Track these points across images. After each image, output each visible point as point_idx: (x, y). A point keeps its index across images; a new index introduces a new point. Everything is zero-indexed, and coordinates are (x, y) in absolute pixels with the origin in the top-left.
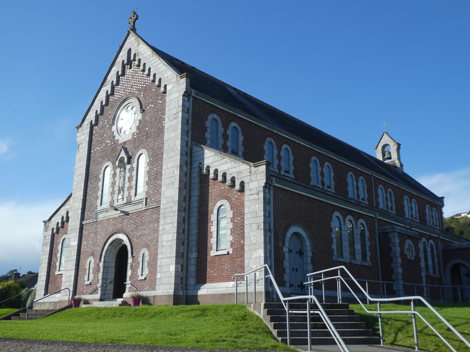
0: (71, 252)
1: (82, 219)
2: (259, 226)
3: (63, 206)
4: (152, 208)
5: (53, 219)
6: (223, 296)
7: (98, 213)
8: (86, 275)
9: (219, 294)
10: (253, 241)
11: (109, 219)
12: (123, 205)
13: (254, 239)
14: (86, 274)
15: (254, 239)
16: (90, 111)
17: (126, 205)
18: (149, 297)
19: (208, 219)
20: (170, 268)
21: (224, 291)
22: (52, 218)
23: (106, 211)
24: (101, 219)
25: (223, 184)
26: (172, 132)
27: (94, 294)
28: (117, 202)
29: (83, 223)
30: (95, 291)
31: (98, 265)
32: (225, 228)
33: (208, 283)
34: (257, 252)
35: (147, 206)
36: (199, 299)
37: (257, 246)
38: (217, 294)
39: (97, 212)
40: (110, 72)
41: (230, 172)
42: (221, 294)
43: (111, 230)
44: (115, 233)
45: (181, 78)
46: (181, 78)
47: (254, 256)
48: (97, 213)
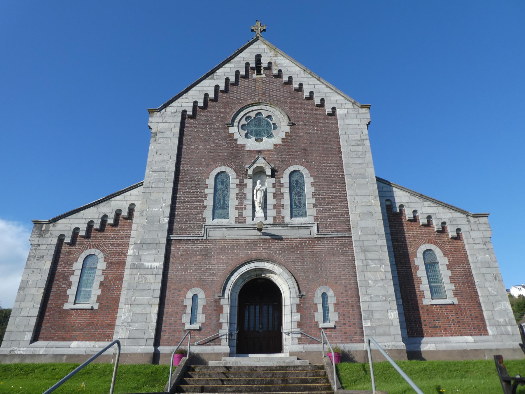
0: (146, 276)
1: (170, 231)
2: (497, 278)
3: (92, 206)
4: (330, 237)
5: (60, 221)
6: (464, 352)
7: (208, 229)
8: (184, 315)
9: (457, 350)
10: (491, 292)
11: (238, 239)
12: (269, 226)
13: (492, 289)
14: (185, 313)
15: (492, 289)
16: (180, 98)
17: (271, 226)
18: (349, 351)
19: (410, 263)
20: (389, 314)
21: (465, 346)
22: (58, 220)
23: (228, 229)
24: (214, 238)
25: (424, 227)
26: (357, 157)
27: (210, 345)
28: (253, 219)
29: (172, 238)
30: (215, 340)
31: (217, 301)
32: (235, 276)
33: (426, 336)
34: (501, 304)
35: (319, 234)
36: (424, 356)
37: (499, 297)
38: (455, 351)
39: (206, 227)
40: (221, 67)
41: (438, 216)
42: (461, 350)
43: (243, 256)
44: (254, 260)
45: (362, 107)
46: (362, 107)
47: (498, 309)
48: (207, 228)
